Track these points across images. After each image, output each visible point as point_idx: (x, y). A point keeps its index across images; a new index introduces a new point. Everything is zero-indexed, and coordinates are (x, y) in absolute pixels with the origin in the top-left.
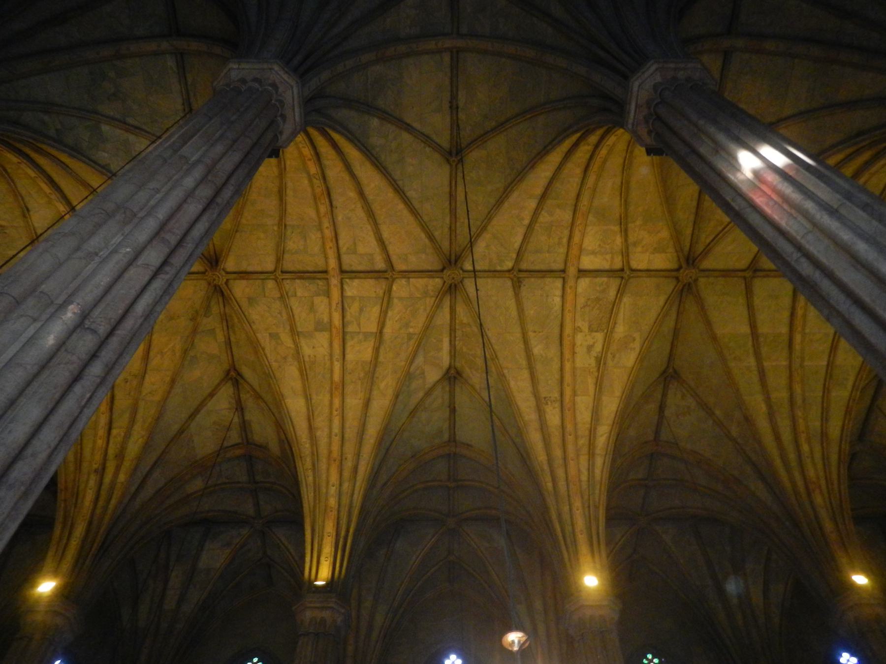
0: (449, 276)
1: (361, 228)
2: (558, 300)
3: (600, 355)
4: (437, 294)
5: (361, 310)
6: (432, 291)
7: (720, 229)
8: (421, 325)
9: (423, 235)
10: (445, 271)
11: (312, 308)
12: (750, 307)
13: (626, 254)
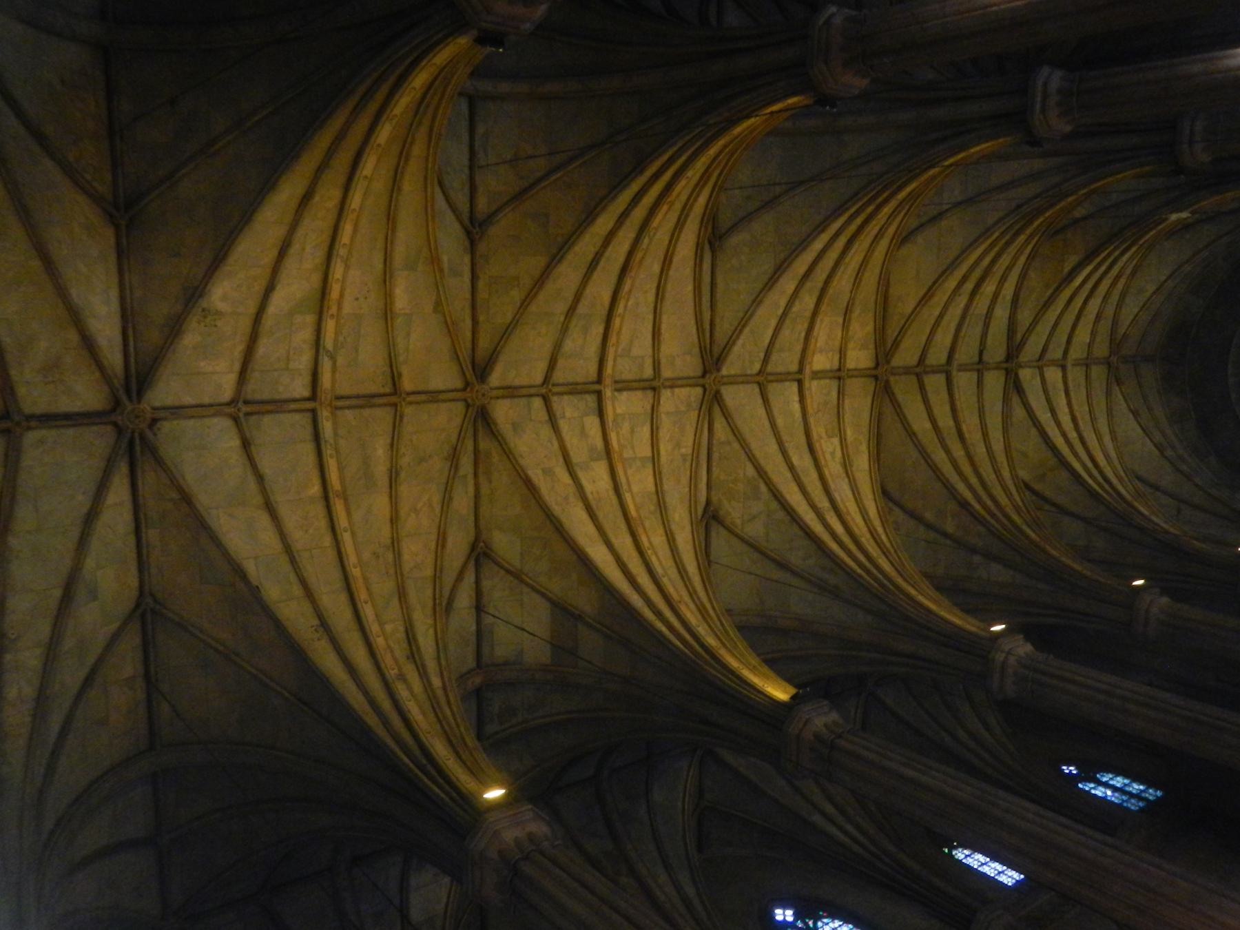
0: (714, 380)
1: (644, 319)
2: (796, 407)
3: (842, 460)
4: (699, 406)
5: (632, 431)
6: (695, 402)
7: (903, 322)
8: (690, 443)
9: (694, 330)
10: (708, 376)
11: (583, 433)
12: (926, 401)
13: (842, 353)
